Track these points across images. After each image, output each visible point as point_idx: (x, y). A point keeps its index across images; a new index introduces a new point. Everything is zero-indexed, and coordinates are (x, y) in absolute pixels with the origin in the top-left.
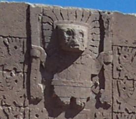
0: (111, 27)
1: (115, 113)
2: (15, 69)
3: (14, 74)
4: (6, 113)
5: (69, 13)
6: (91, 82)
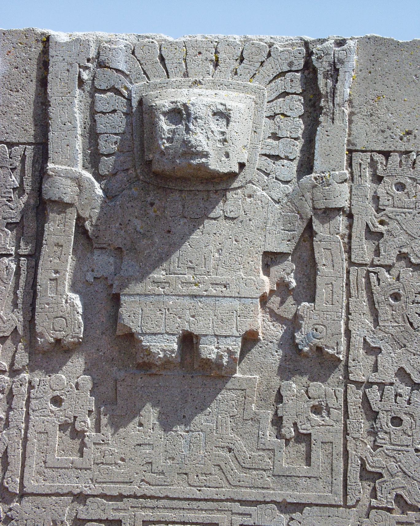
1: (358, 384)
5: (191, 51)
6: (265, 278)
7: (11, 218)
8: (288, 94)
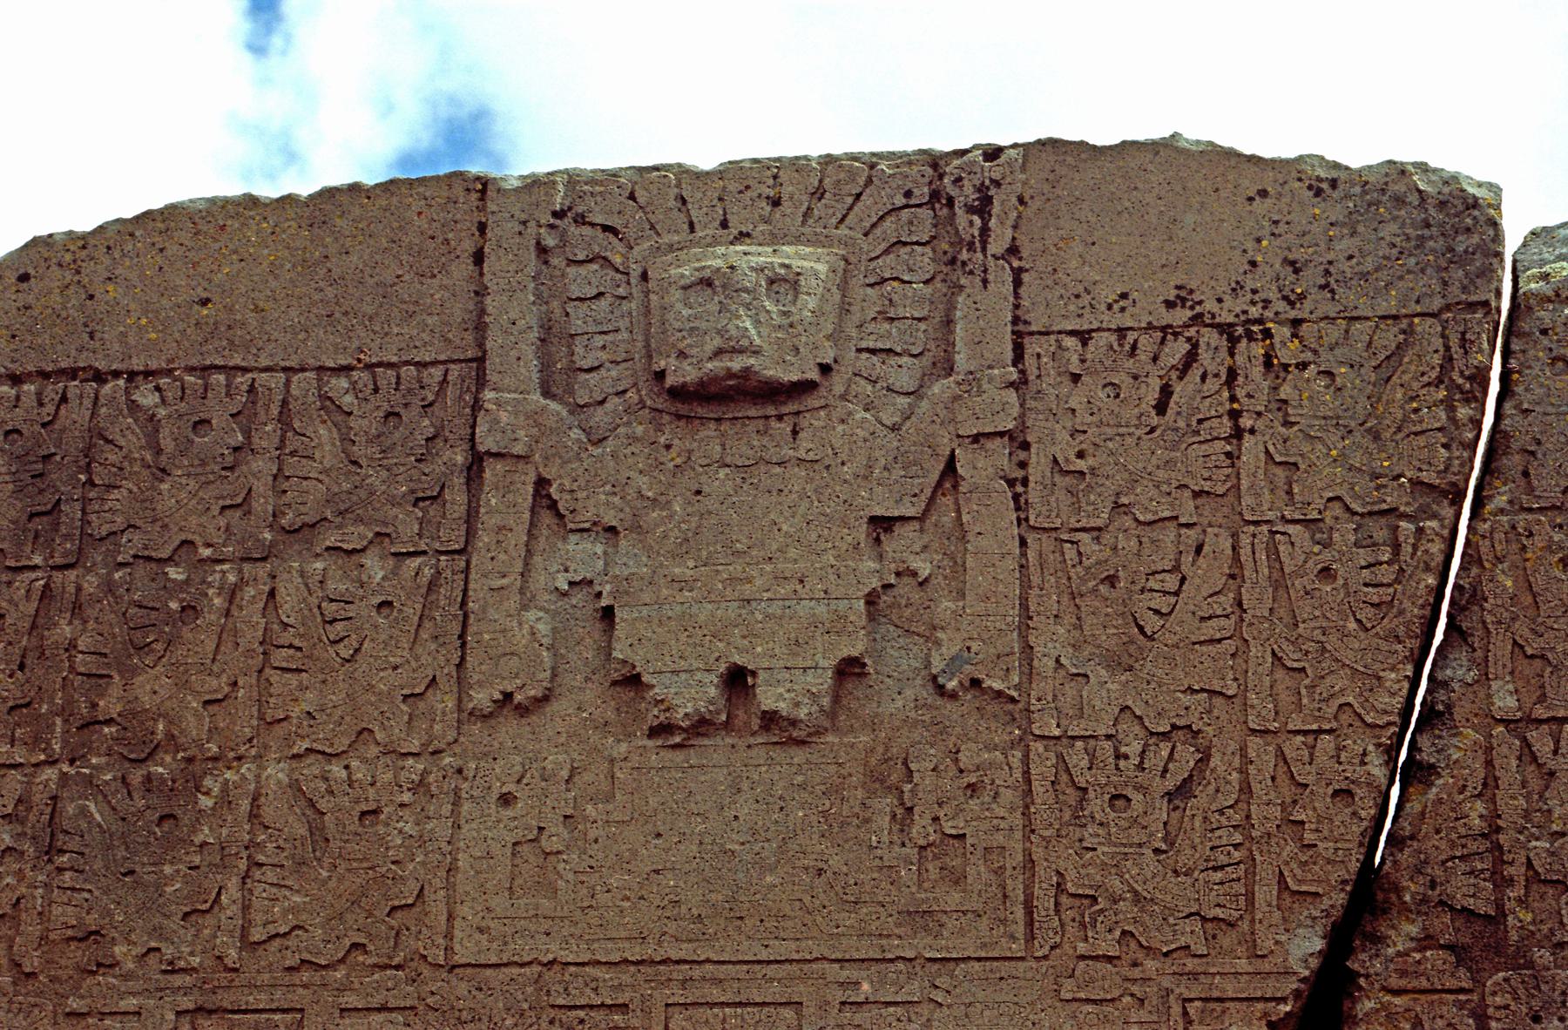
7: (423, 490)
8: (905, 244)
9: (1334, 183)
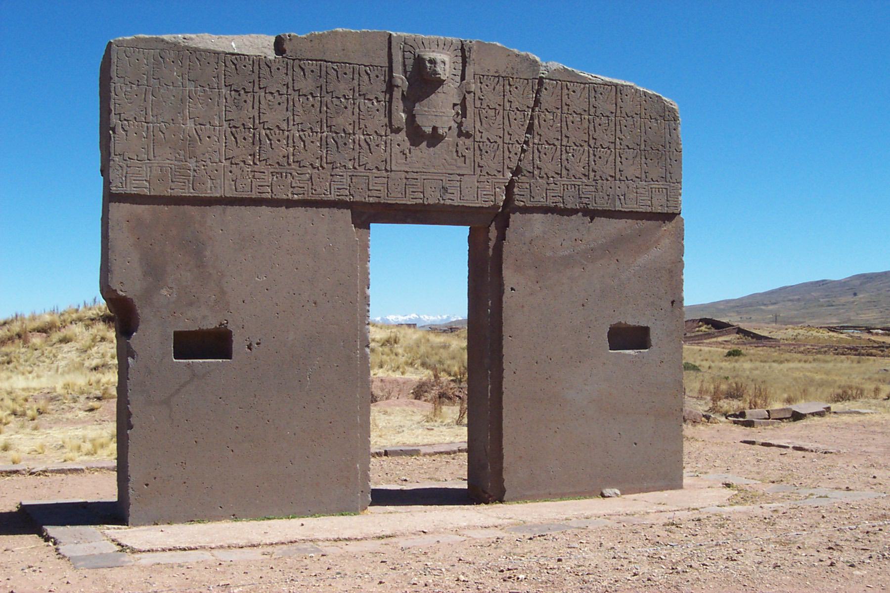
0: (473, 56)
1: (477, 142)
2: (376, 98)
3: (375, 104)
4: (367, 142)
9: (519, 55)
